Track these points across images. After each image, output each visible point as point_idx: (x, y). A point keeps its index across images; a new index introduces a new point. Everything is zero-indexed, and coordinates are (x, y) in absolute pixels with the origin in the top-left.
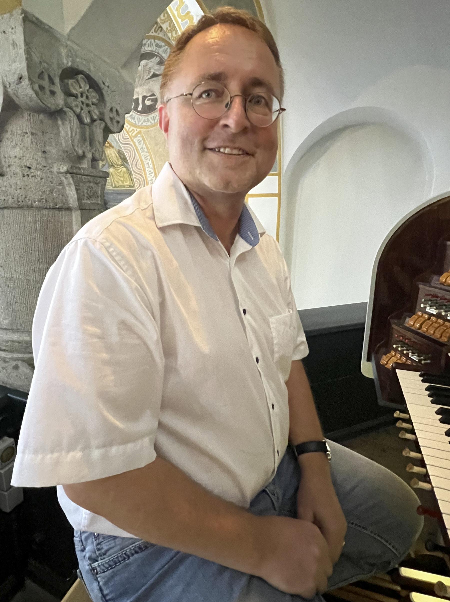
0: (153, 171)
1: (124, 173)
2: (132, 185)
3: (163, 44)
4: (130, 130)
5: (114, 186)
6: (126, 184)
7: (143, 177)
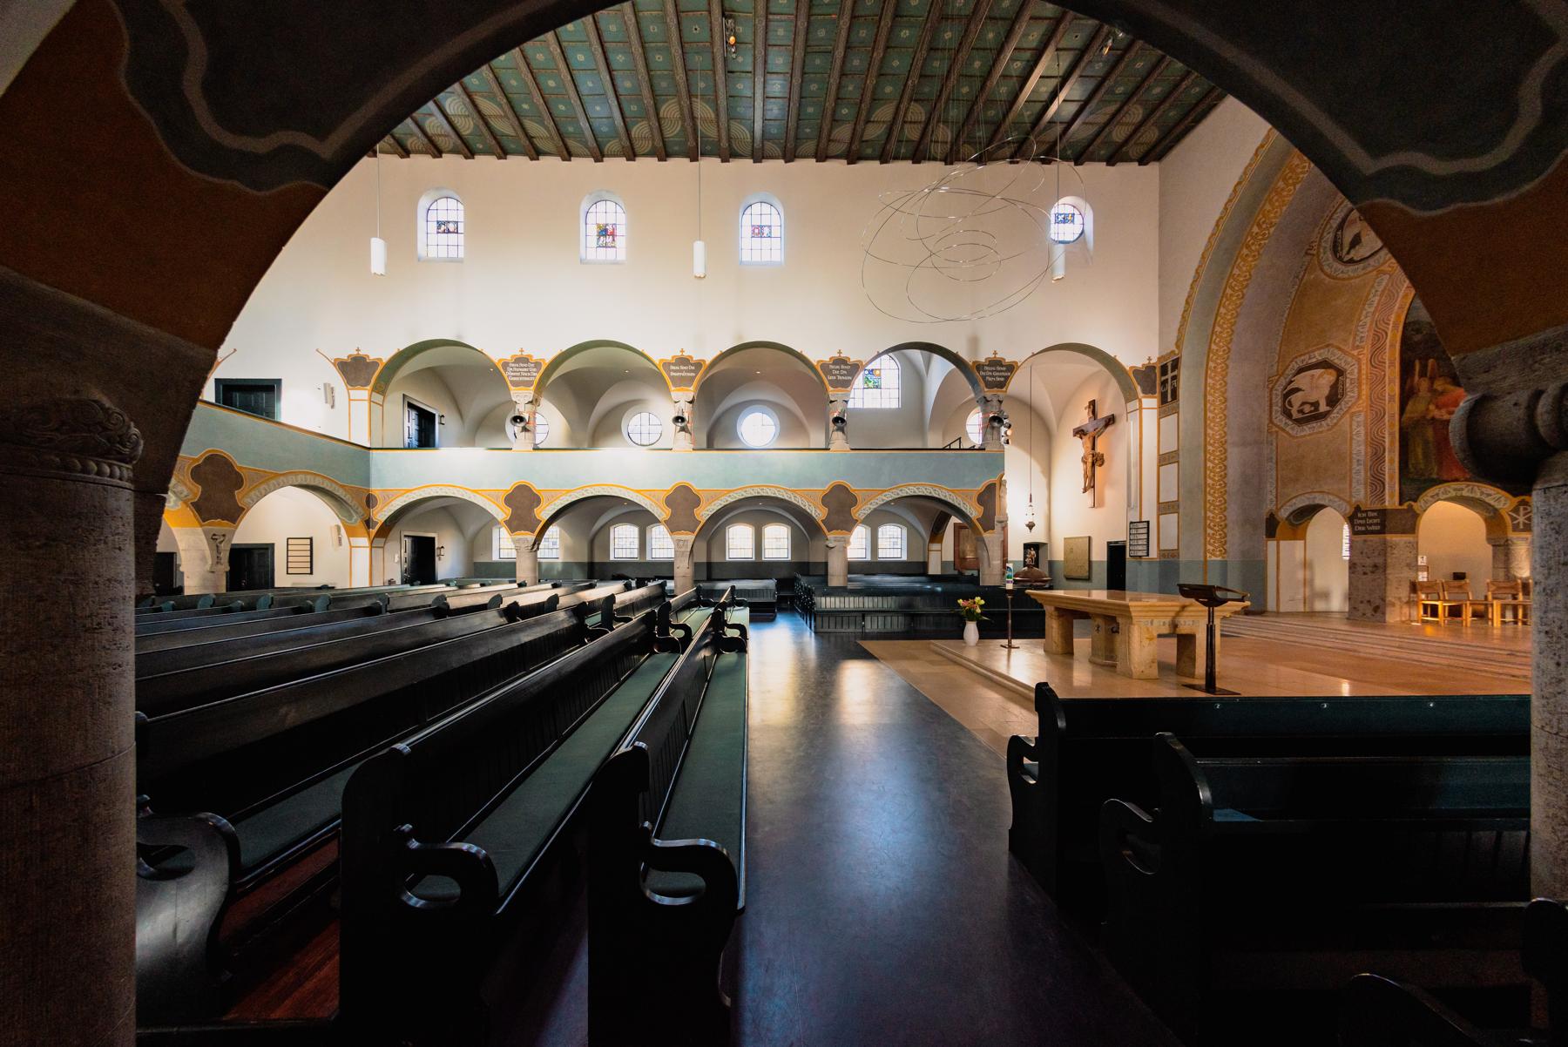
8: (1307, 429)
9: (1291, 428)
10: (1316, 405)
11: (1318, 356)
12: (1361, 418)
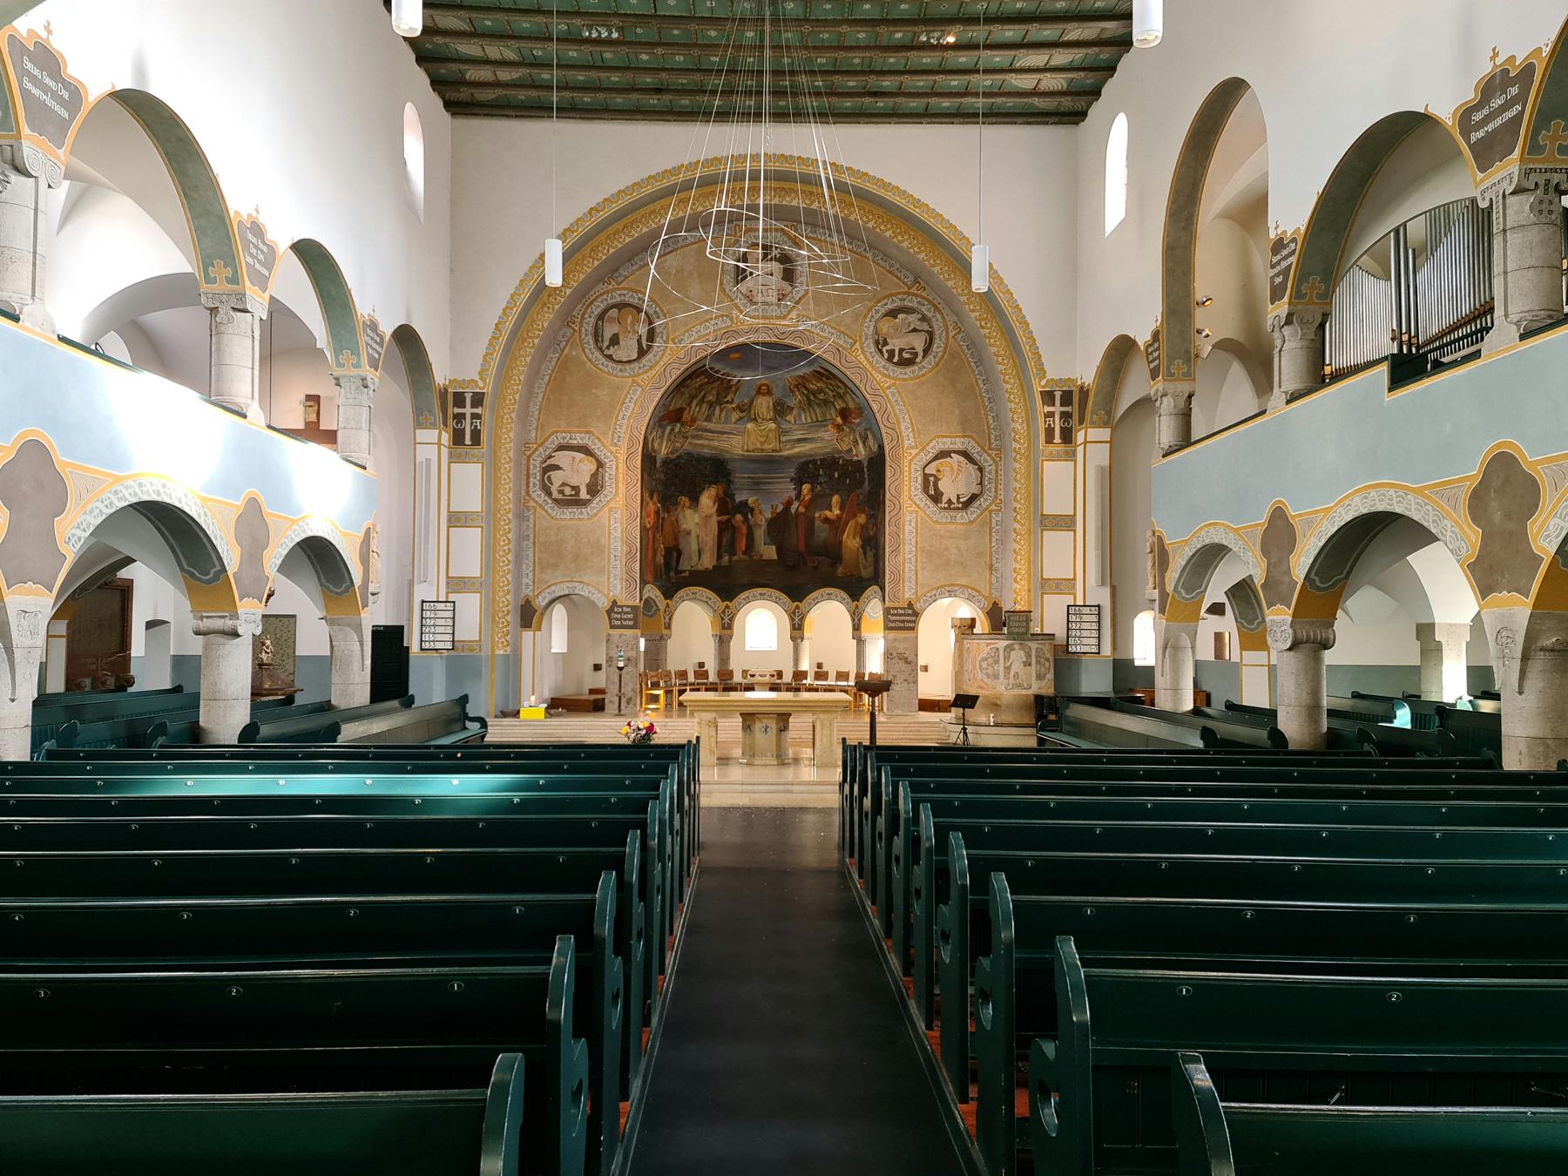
8: (567, 513)
9: (550, 504)
10: (576, 489)
12: (618, 515)
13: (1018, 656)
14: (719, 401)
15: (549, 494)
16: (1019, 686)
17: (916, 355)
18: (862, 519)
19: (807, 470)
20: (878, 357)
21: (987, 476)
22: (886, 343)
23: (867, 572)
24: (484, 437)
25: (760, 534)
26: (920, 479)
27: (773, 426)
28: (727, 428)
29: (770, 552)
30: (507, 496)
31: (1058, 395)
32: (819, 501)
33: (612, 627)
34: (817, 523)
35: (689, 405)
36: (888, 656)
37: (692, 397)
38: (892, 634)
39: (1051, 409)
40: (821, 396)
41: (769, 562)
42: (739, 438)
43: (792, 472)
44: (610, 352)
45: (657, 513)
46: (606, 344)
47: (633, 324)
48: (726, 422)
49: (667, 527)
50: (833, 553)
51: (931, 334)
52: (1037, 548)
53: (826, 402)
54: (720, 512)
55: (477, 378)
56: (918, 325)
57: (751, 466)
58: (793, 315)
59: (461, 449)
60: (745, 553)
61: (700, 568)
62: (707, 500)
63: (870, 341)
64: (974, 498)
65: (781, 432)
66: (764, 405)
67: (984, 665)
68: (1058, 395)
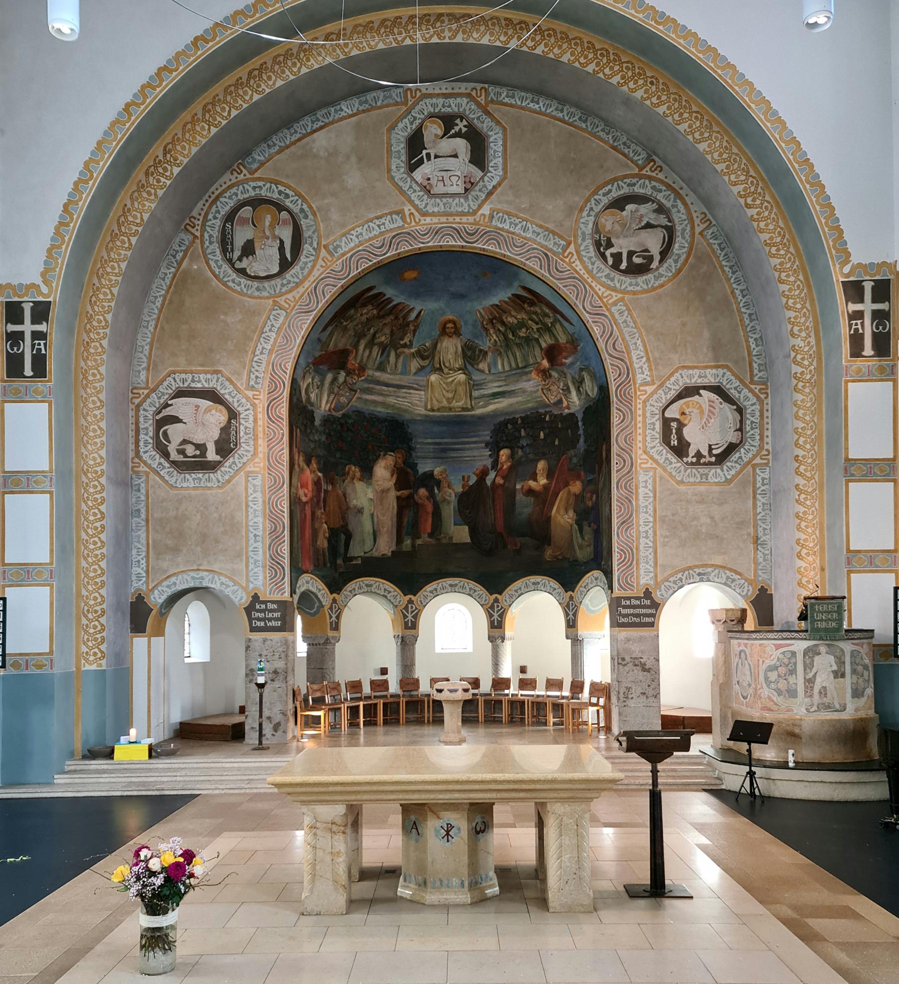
0: (643, 354)
1: (459, 383)
2: (469, 407)
3: (664, 188)
4: (605, 295)
5: (429, 407)
6: (455, 404)
7: (626, 363)
8: (191, 480)
9: (166, 470)
10: (202, 448)
11: (203, 382)
12: (258, 482)
13: (825, 662)
14: (394, 344)
15: (166, 455)
16: (828, 707)
17: (650, 259)
18: (576, 487)
19: (505, 432)
20: (599, 263)
21: (749, 419)
22: (609, 245)
23: (583, 554)
24: (52, 365)
25: (449, 512)
26: (658, 426)
27: (462, 377)
28: (404, 380)
29: (462, 534)
30: (97, 454)
31: (868, 287)
32: (521, 468)
33: (253, 629)
34: (519, 497)
35: (356, 346)
36: (618, 660)
37: (359, 336)
38: (624, 633)
39: (859, 307)
40: (522, 333)
41: (460, 547)
42: (422, 393)
43: (486, 435)
44: (244, 264)
45: (317, 483)
46: (237, 254)
47: (272, 227)
48: (405, 372)
49: (332, 503)
50: (540, 531)
51: (670, 231)
52: (837, 511)
53: (528, 340)
54: (399, 486)
55: (38, 281)
56: (652, 218)
57: (436, 429)
58: (486, 210)
59: (18, 383)
60: (431, 535)
61: (375, 554)
62: (383, 471)
63: (589, 241)
64: (731, 448)
65: (473, 385)
66: (450, 349)
67: (773, 676)
68: (868, 287)
